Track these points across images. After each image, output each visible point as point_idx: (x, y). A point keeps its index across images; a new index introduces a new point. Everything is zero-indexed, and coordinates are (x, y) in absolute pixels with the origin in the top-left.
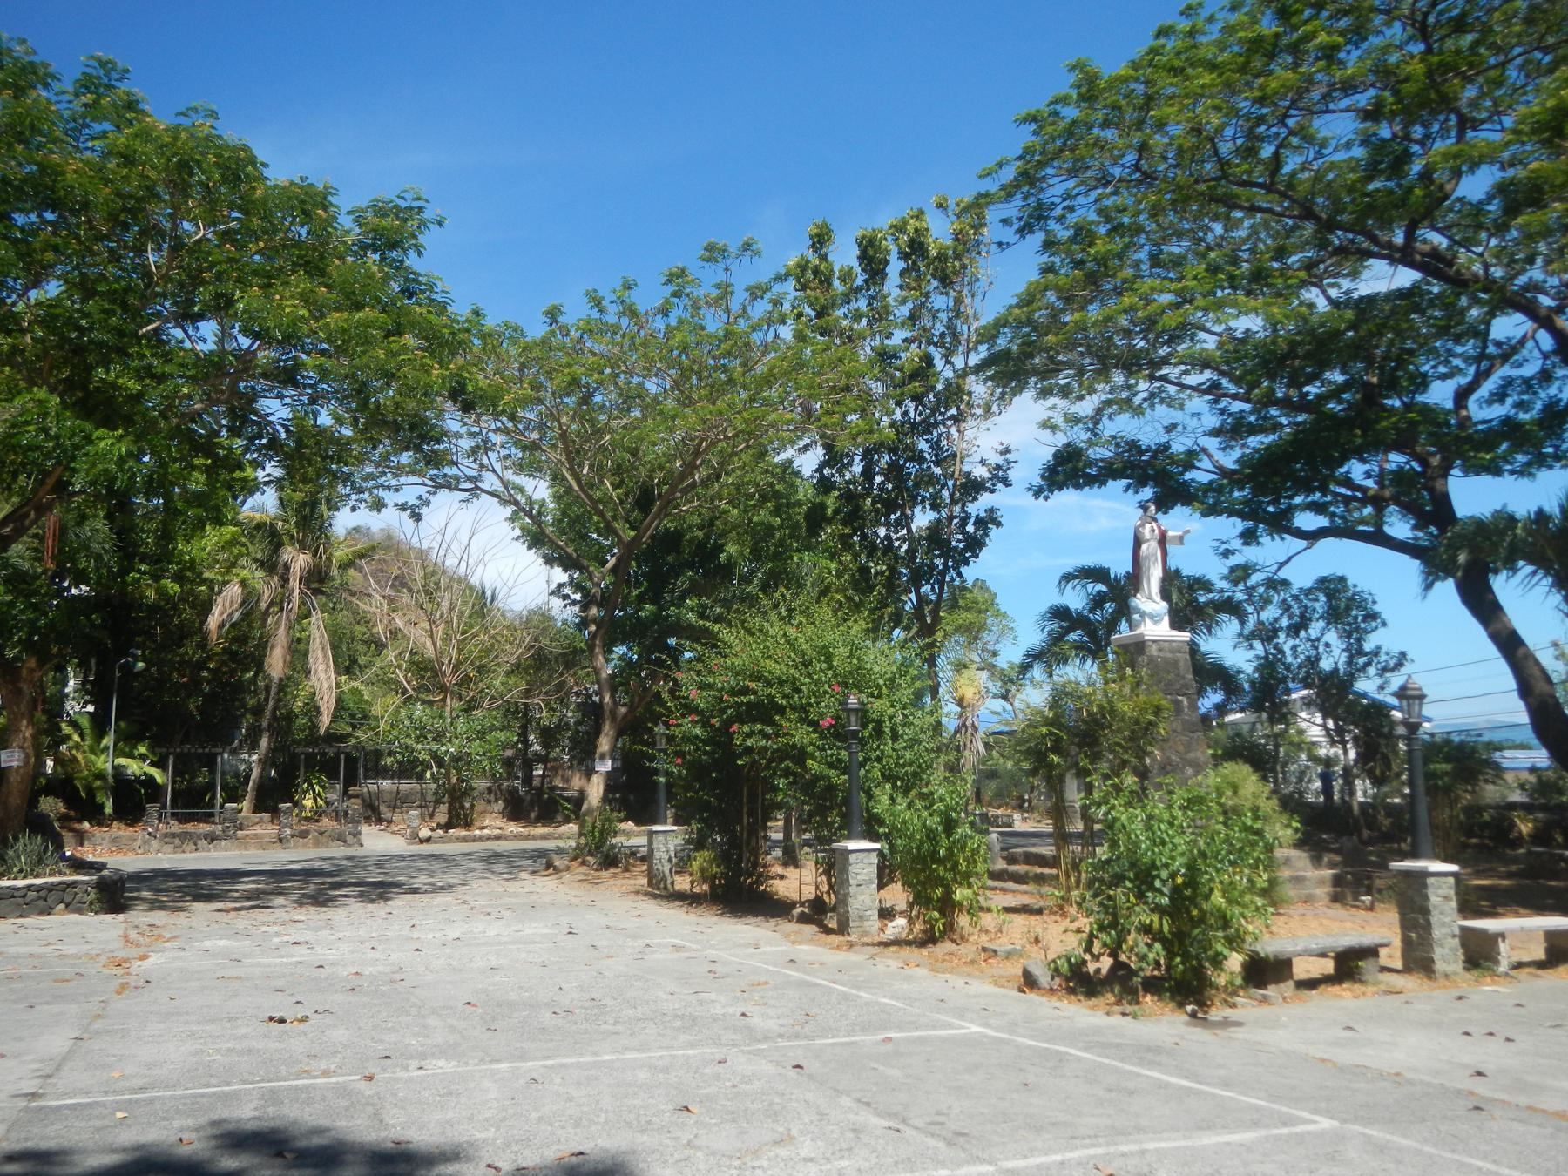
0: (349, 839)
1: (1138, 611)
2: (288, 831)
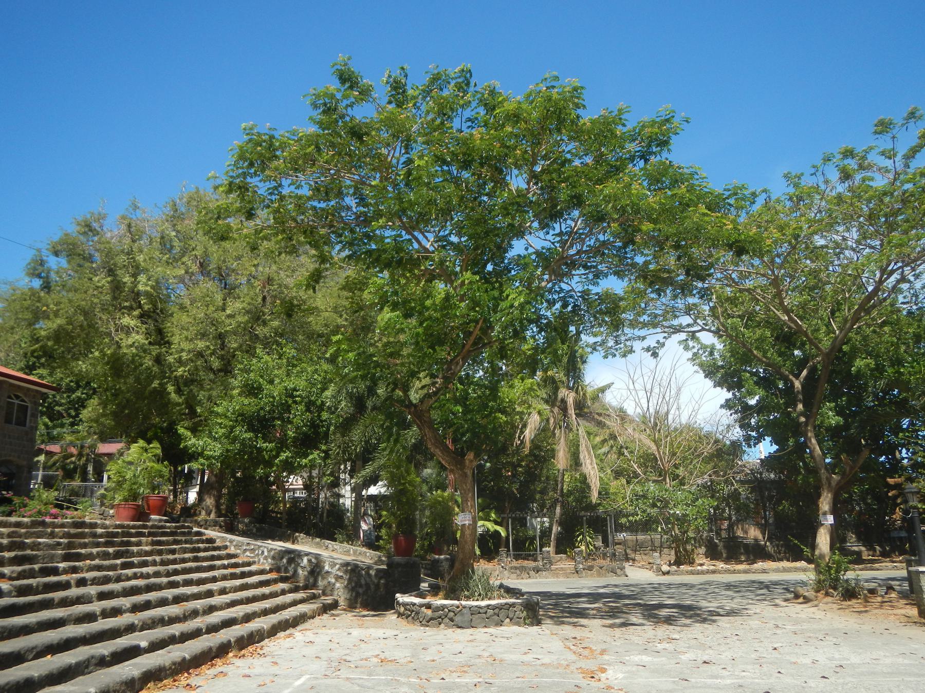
0: (618, 571)
2: (581, 566)
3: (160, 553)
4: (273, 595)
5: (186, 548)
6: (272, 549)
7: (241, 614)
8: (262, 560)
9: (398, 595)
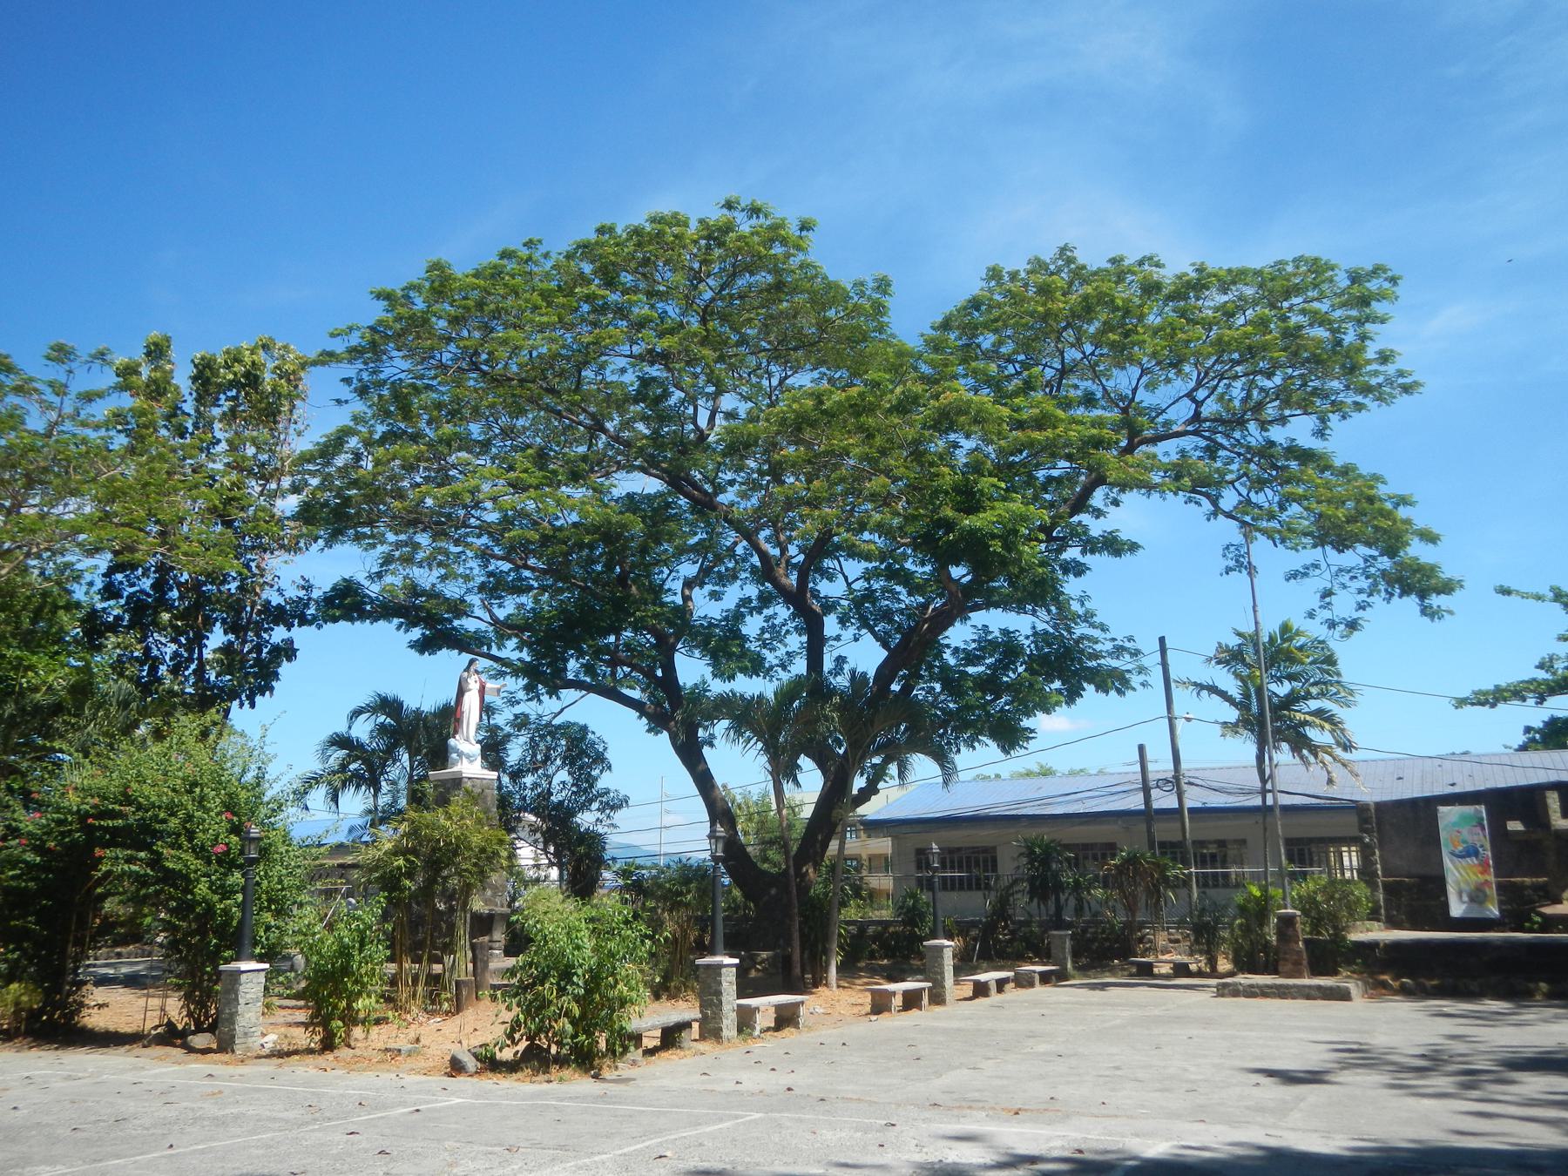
1: (457, 751)
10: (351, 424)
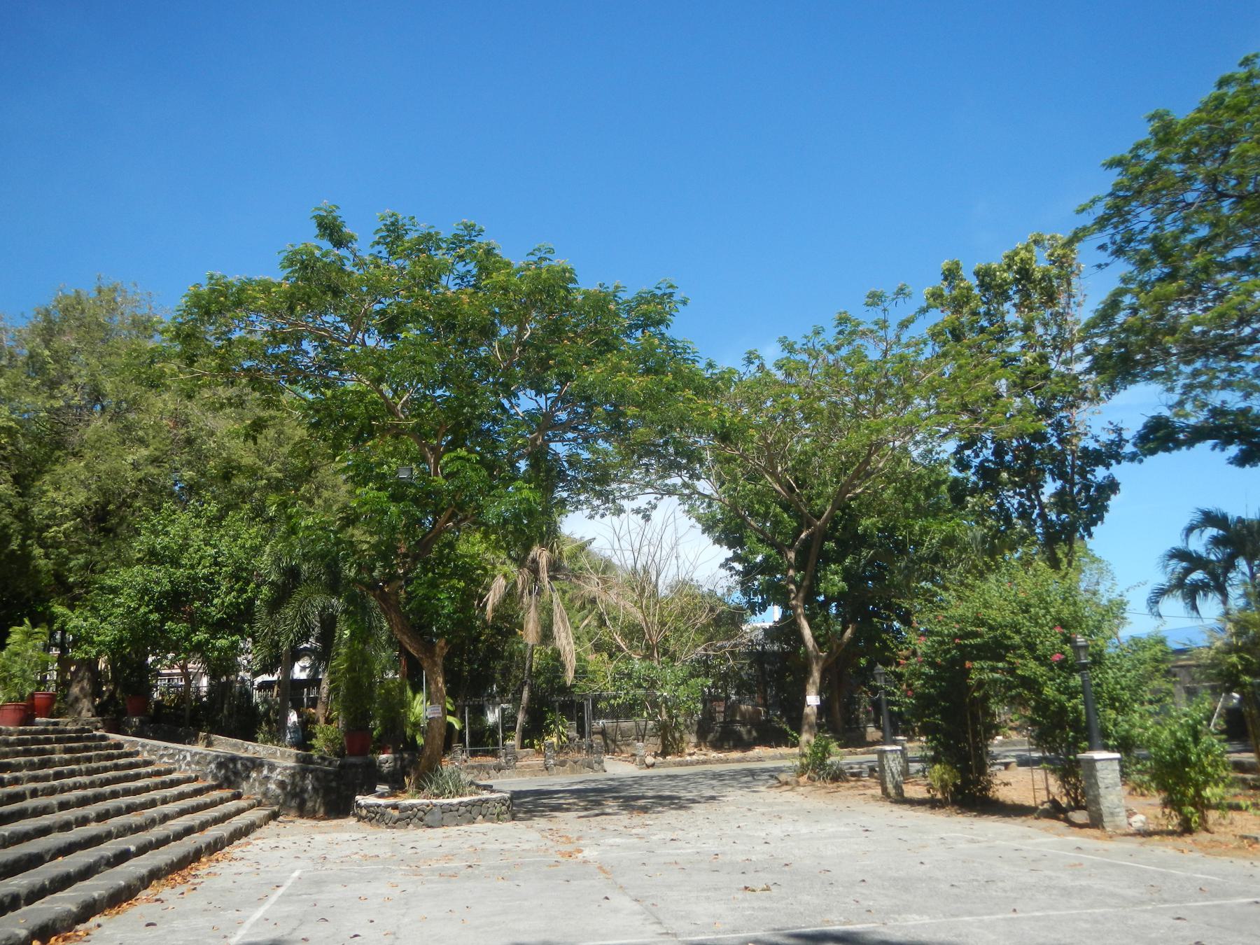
0: (596, 766)
2: (552, 762)
3: (78, 761)
4: (213, 804)
5: (101, 755)
6: (196, 753)
7: (198, 822)
8: (183, 767)
9: (358, 797)
10: (1122, 285)
